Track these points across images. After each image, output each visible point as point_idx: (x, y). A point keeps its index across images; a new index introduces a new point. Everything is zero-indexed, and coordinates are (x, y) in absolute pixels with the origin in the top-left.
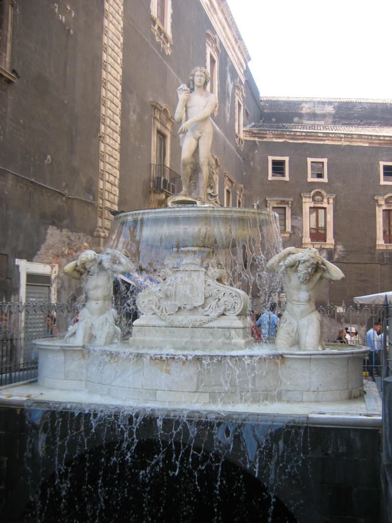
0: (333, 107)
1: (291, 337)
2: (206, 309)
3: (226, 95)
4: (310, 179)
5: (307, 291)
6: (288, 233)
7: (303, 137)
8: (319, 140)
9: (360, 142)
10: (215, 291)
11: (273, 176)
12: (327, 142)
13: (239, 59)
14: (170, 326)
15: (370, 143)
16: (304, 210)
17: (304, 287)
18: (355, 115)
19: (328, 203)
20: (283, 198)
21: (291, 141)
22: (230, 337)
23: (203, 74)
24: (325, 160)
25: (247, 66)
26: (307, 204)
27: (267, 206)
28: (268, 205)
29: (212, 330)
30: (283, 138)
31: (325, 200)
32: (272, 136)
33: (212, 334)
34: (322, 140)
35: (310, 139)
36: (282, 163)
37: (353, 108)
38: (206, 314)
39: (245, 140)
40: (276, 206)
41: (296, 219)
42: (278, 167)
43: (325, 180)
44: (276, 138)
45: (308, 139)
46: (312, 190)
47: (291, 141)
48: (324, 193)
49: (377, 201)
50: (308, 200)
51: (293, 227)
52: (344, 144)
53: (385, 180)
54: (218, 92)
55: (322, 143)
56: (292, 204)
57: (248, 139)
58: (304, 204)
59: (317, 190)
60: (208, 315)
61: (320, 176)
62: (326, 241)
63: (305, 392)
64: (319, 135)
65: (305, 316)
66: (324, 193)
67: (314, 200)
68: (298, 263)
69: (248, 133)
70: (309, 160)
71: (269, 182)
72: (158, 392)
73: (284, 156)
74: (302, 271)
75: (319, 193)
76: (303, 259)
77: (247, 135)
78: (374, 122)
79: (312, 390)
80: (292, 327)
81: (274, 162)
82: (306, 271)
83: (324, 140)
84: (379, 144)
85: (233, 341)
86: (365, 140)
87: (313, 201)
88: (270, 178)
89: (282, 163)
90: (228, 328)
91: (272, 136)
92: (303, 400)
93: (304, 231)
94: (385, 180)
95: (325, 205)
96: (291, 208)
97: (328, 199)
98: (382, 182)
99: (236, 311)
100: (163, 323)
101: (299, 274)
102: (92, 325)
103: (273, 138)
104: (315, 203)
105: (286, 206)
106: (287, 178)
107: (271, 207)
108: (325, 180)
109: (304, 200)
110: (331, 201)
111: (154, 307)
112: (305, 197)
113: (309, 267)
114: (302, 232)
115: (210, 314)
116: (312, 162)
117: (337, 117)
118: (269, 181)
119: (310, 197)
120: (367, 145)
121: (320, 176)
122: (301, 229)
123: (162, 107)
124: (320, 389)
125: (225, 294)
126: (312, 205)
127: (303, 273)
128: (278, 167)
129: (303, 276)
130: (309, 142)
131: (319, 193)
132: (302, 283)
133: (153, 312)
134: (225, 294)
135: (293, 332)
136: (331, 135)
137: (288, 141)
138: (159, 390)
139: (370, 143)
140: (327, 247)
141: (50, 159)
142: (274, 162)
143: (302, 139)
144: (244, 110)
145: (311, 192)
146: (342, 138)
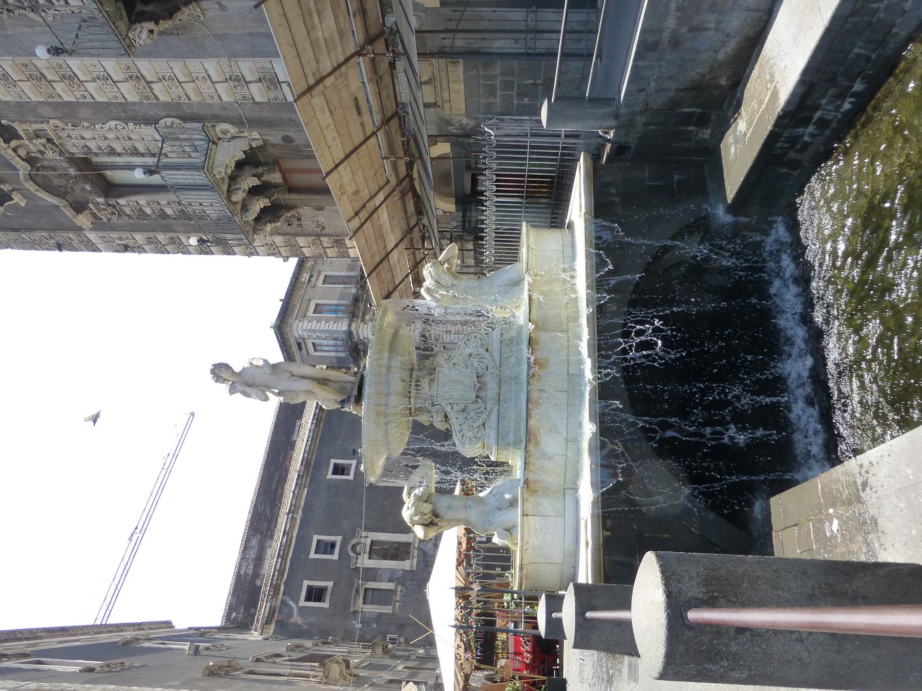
0: (252, 538)
4: (335, 556)
6: (396, 586)
12: (295, 534)
18: (268, 512)
19: (367, 537)
20: (354, 590)
24: (316, 538)
26: (365, 562)
30: (279, 586)
31: (363, 540)
35: (288, 553)
36: (310, 589)
37: (259, 514)
40: (361, 600)
41: (380, 575)
42: (315, 594)
43: (338, 539)
44: (278, 594)
45: (287, 556)
46: (348, 554)
48: (354, 541)
50: (359, 561)
51: (390, 581)
53: (348, 474)
57: (272, 631)
59: (349, 548)
61: (333, 545)
62: (411, 543)
66: (354, 541)
69: (264, 630)
70: (312, 555)
71: (332, 607)
72: (570, 372)
77: (267, 632)
78: (280, 491)
81: (308, 599)
83: (292, 537)
84: (306, 477)
86: (300, 492)
89: (310, 589)
93: (396, 567)
94: (348, 474)
95: (369, 542)
100: (495, 409)
103: (277, 599)
106: (330, 584)
107: (363, 606)
108: (338, 539)
111: (477, 424)
114: (398, 570)
117: (266, 533)
118: (330, 606)
119: (357, 558)
120: (306, 490)
121: (333, 545)
122: (393, 571)
126: (367, 556)
128: (315, 594)
130: (290, 555)
131: (354, 548)
133: (482, 427)
136: (287, 528)
137: (284, 580)
138: (568, 371)
139: (305, 487)
142: (308, 599)
143: (285, 563)
145: (350, 557)
146: (293, 517)
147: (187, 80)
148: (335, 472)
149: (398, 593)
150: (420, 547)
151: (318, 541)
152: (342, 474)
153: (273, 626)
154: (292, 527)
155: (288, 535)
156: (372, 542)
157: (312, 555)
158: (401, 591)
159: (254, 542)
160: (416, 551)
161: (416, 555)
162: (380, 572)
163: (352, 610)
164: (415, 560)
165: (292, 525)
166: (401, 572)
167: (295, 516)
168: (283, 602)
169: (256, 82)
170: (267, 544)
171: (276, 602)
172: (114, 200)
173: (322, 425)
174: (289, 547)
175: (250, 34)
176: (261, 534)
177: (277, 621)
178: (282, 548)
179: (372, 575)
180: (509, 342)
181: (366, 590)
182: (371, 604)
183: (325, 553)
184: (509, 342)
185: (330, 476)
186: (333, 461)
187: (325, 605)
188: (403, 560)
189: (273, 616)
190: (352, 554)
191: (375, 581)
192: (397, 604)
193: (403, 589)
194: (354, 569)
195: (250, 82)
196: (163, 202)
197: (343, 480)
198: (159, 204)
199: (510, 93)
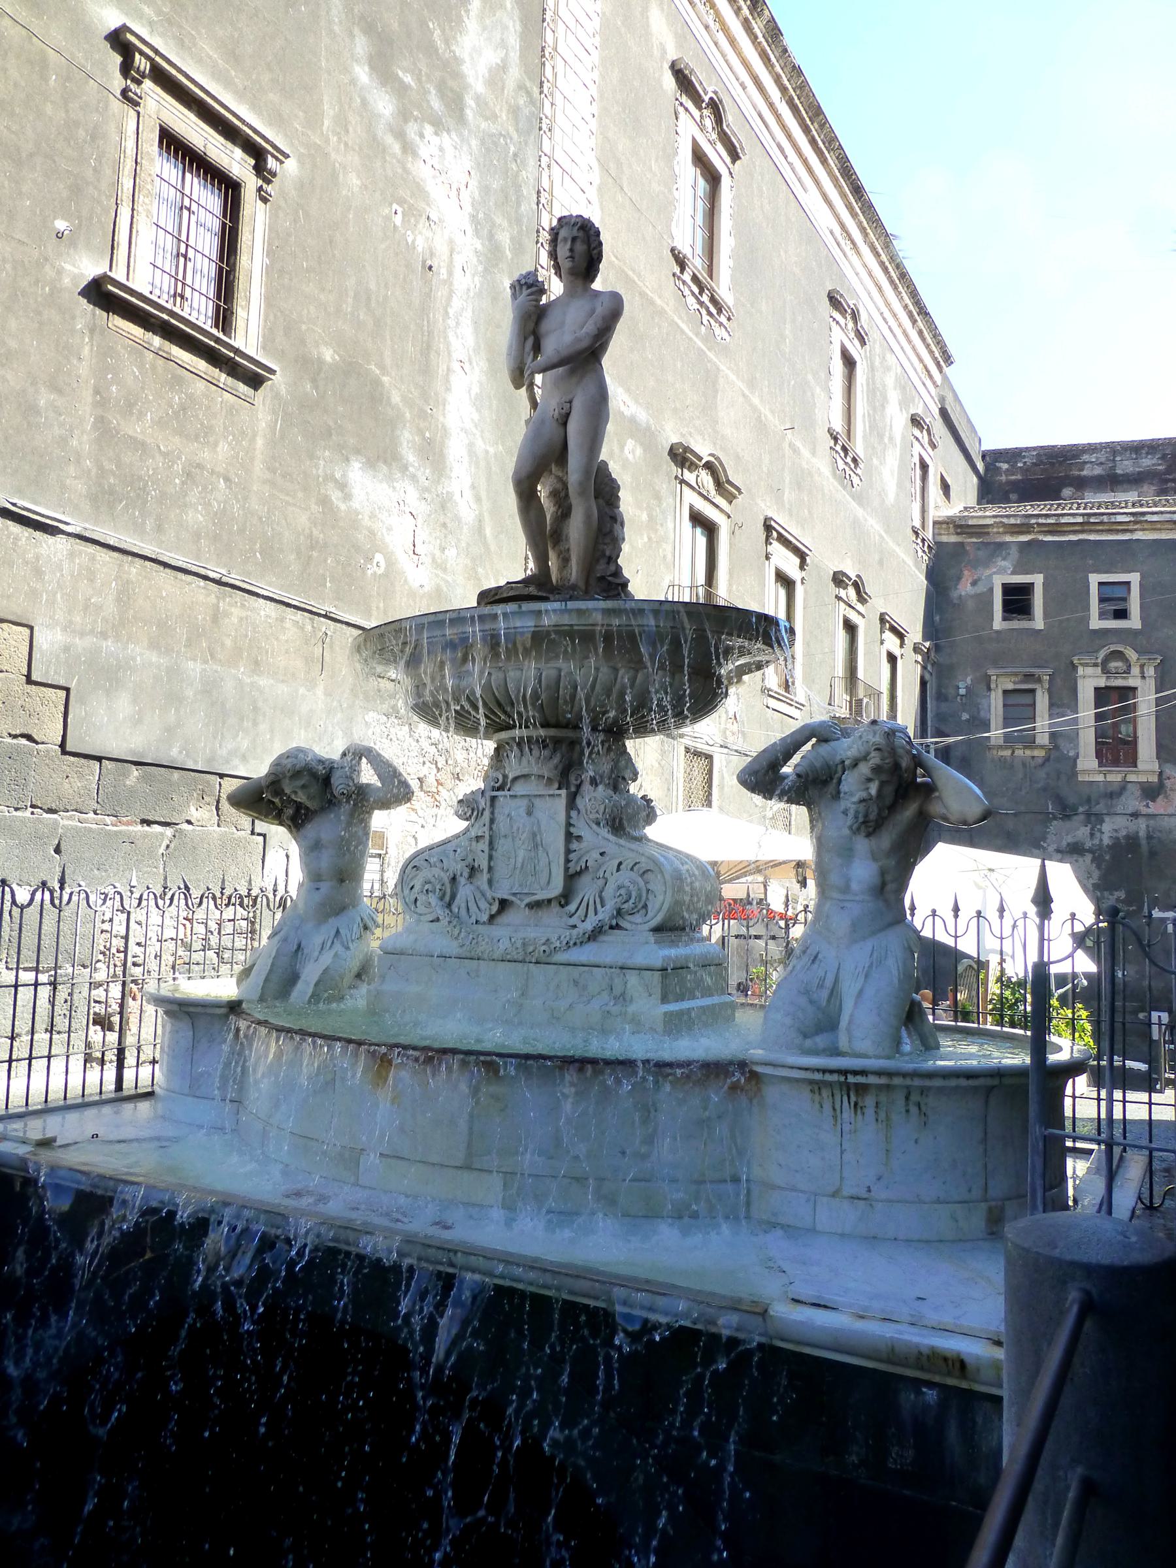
1: (811, 1002)
2: (572, 907)
3: (886, 440)
4: (1096, 623)
5: (875, 859)
6: (1042, 747)
7: (1077, 528)
8: (1117, 531)
10: (595, 855)
11: (1004, 619)
12: (1139, 535)
13: (921, 360)
14: (468, 955)
16: (1080, 696)
17: (862, 845)
19: (1143, 677)
20: (1028, 670)
21: (1049, 538)
22: (622, 998)
23: (581, 234)
25: (945, 378)
26: (1089, 681)
27: (989, 689)
28: (993, 686)
29: (576, 972)
30: (1029, 532)
31: (1135, 670)
32: (1001, 530)
33: (576, 983)
35: (1097, 531)
36: (1027, 589)
38: (572, 921)
40: (1010, 686)
44: (1013, 533)
45: (1091, 531)
47: (1049, 538)
48: (1132, 655)
50: (1090, 671)
54: (865, 431)
55: (1126, 537)
56: (1050, 681)
58: (1080, 683)
59: (1113, 648)
60: (575, 926)
61: (1122, 614)
63: (825, 1199)
64: (1120, 518)
65: (864, 938)
66: (1132, 655)
67: (1106, 671)
68: (840, 768)
69: (944, 526)
70: (1094, 579)
71: (994, 635)
73: (1032, 573)
74: (852, 795)
75: (1118, 655)
76: (849, 753)
79: (847, 1191)
80: (821, 973)
82: (864, 795)
85: (631, 1009)
87: (1102, 670)
88: (998, 623)
89: (1027, 589)
90: (622, 968)
91: (1001, 530)
92: (819, 1227)
93: (1082, 743)
96: (1050, 691)
97: (1142, 667)
99: (650, 914)
101: (844, 804)
102: (299, 946)
103: (1005, 533)
106: (1039, 622)
108: (1134, 622)
109: (1080, 671)
110: (1150, 671)
112: (1086, 665)
113: (869, 780)
114: (1077, 746)
115: (579, 924)
116: (1100, 584)
119: (1096, 665)
121: (1122, 614)
122: (1074, 737)
123: (700, 459)
124: (879, 1193)
125: (620, 864)
126: (1102, 682)
127: (855, 799)
129: (857, 812)
130: (1092, 537)
131: (1118, 655)
132: (856, 831)
134: (620, 864)
135: (821, 986)
136: (1149, 518)
137: (1041, 537)
140: (1142, 778)
141: (383, 564)
143: (1075, 532)
144: (935, 475)
145: (1097, 651)
149: (1028, 753)
150: (1129, 785)
153: (953, 539)
154: (1154, 526)
155: (1136, 522)
157: (1094, 579)
158: (1033, 757)
159: (1148, 462)
160: (1119, 778)
161: (1110, 778)
163: (990, 672)
164: (1100, 778)
165: (1159, 526)
166: (1071, 754)
168: (1001, 546)
170: (1146, 487)
171: (998, 533)
174: (1110, 531)
176: (1168, 471)
177: (962, 544)
178: (1105, 519)
179: (1064, 699)
180: (618, 990)
182: (1005, 705)
183: (1102, 600)
184: (618, 990)
187: (998, 623)
188: (1099, 755)
189: (971, 535)
190: (1102, 654)
192: (1007, 753)
193: (1040, 761)
194: (1072, 662)
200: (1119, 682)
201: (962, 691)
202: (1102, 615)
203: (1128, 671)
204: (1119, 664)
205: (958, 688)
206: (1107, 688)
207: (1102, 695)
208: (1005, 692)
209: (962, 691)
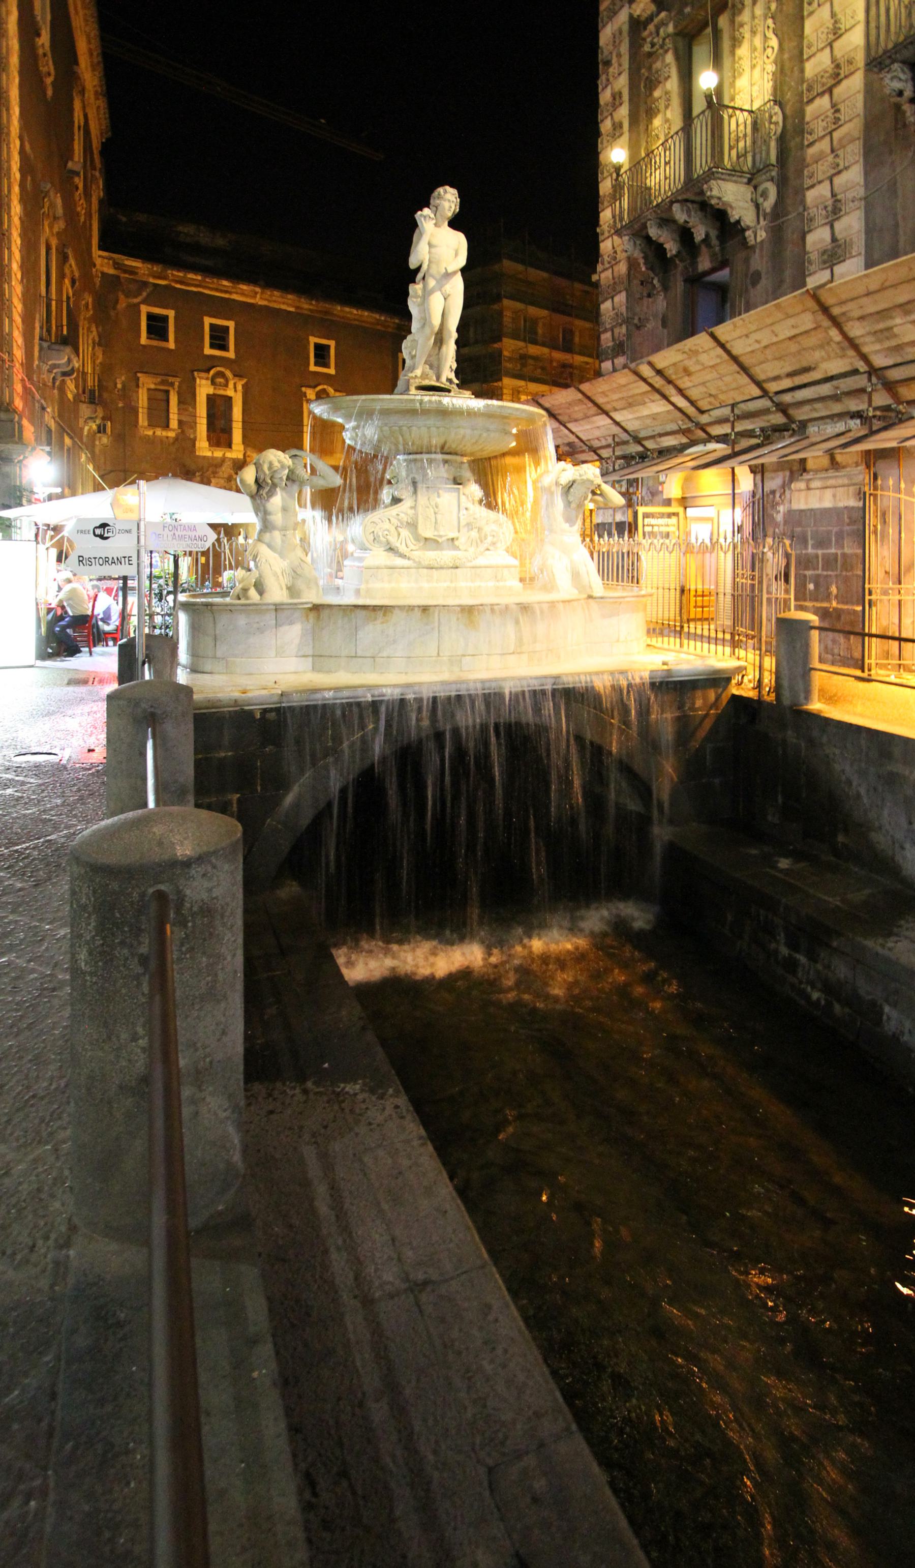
4: (208, 351)
6: (174, 430)
8: (221, 291)
9: (284, 303)
11: (148, 338)
15: (297, 308)
16: (198, 398)
19: (236, 391)
21: (178, 286)
24: (231, 324)
26: (204, 389)
27: (138, 386)
28: (141, 385)
31: (231, 384)
34: (226, 292)
39: (103, 273)
40: (153, 386)
41: (186, 410)
43: (231, 354)
44: (155, 277)
47: (178, 286)
48: (229, 374)
49: (305, 394)
50: (204, 382)
51: (180, 422)
52: (260, 303)
53: (316, 364)
55: (226, 296)
66: (229, 374)
69: (106, 261)
70: (208, 321)
75: (221, 374)
81: (151, 317)
83: (230, 293)
88: (144, 340)
94: (316, 364)
95: (230, 392)
96: (179, 394)
98: (313, 368)
104: (215, 389)
105: (171, 389)
108: (231, 354)
109: (198, 381)
110: (239, 388)
112: (201, 378)
114: (195, 432)
119: (207, 379)
126: (211, 391)
128: (157, 327)
131: (221, 374)
137: (173, 284)
143: (196, 286)
147: (835, 143)
148: (318, 347)
149: (164, 433)
151: (227, 328)
152: (316, 356)
153: (112, 271)
156: (230, 398)
157: (208, 321)
158: (167, 437)
162: (191, 409)
164: (209, 454)
166: (192, 436)
167: (258, 296)
168: (145, 284)
169: (833, 234)
172: (670, 46)
173: (379, 327)
175: (897, 225)
177: (118, 277)
179: (188, 398)
181: (167, 392)
182: (149, 399)
183: (211, 337)
185: (313, 340)
186: (332, 344)
187: (144, 340)
188: (209, 439)
189: (125, 272)
191: (180, 402)
192: (150, 433)
193: (171, 441)
195: (832, 227)
196: (669, 114)
197: (308, 358)
198: (667, 107)
199: (820, 566)
200: (221, 392)
201: (119, 386)
202: (212, 346)
203: (226, 385)
204: (222, 380)
205: (116, 384)
206: (214, 395)
207: (211, 399)
208: (149, 390)
209: (119, 386)
